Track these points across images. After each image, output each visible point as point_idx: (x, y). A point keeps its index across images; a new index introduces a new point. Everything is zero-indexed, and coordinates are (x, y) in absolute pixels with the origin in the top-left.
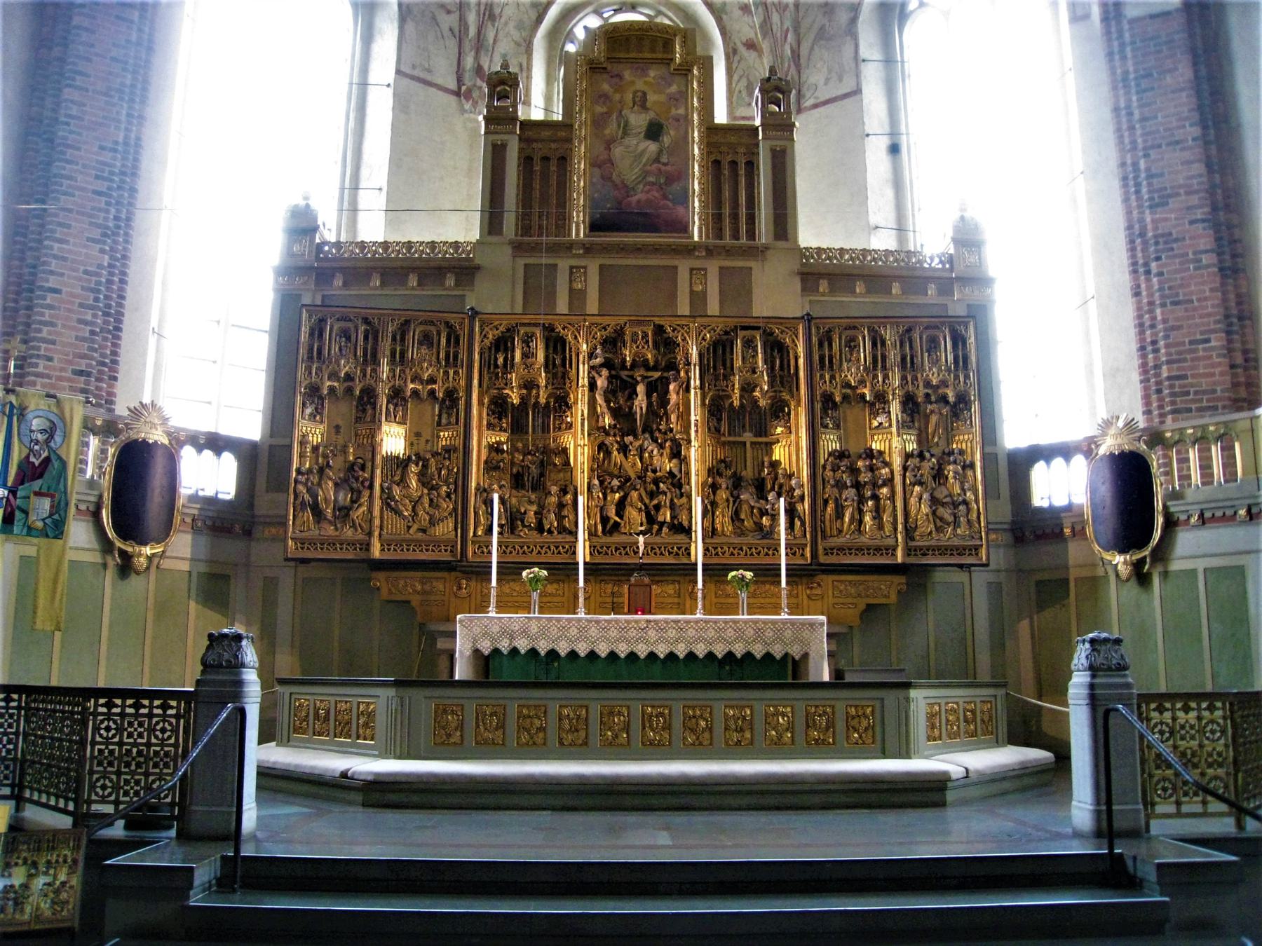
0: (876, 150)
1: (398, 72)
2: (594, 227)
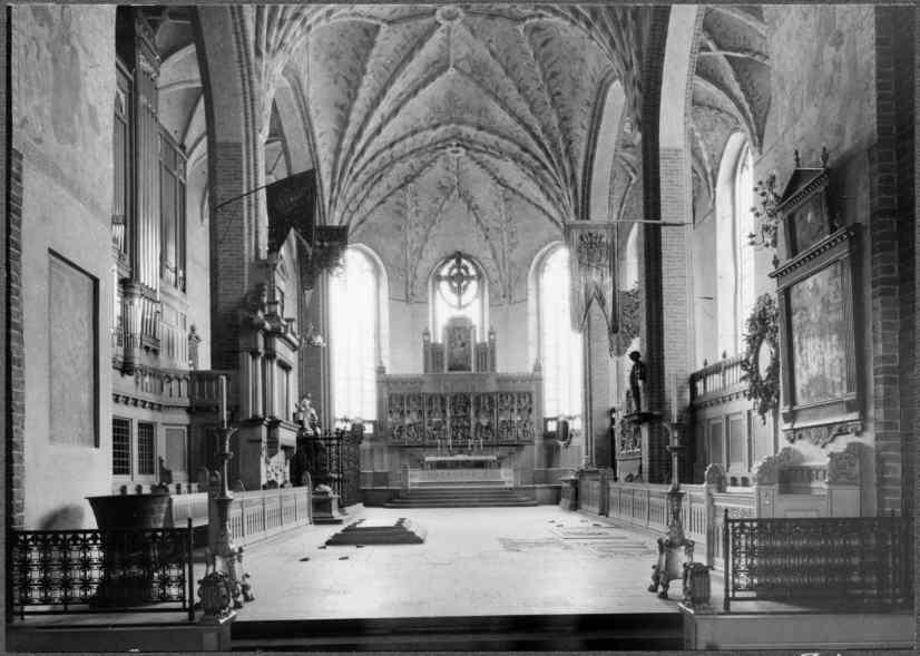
0: (532, 320)
1: (390, 298)
2: (450, 369)
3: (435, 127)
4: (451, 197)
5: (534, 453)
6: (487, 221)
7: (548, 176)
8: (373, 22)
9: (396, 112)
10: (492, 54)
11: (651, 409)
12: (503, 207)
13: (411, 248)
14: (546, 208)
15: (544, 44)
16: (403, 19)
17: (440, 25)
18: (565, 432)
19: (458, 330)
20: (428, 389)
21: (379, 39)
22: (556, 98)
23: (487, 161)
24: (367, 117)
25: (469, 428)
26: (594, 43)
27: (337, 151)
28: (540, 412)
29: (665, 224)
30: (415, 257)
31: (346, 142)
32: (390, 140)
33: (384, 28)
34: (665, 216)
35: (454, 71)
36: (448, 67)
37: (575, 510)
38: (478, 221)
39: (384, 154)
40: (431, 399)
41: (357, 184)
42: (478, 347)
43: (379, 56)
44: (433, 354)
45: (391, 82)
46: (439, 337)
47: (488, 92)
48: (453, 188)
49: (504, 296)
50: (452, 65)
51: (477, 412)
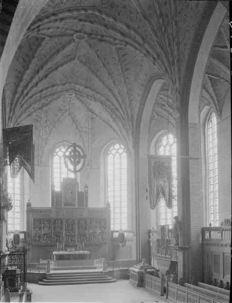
2: (65, 205)
3: (64, 84)
4: (65, 115)
6: (81, 127)
7: (119, 114)
8: (43, 36)
9: (46, 76)
10: (98, 57)
11: (184, 244)
12: (90, 121)
13: (41, 138)
14: (111, 124)
15: (123, 55)
16: (56, 36)
17: (74, 40)
19: (69, 185)
20: (53, 216)
21: (43, 43)
22: (127, 80)
23: (85, 100)
24: (32, 78)
25: (74, 236)
26: (155, 67)
27: (15, 92)
29: (191, 159)
30: (44, 143)
31: (20, 90)
32: (40, 89)
33: (47, 38)
34: (191, 154)
35: (78, 60)
36: (74, 59)
37: (140, 287)
38: (77, 127)
39: (37, 95)
40: (56, 221)
41: (22, 109)
43: (42, 50)
44: (56, 198)
45: (46, 63)
46: (58, 189)
47: (93, 72)
48: (66, 111)
49: (88, 165)
50: (77, 58)
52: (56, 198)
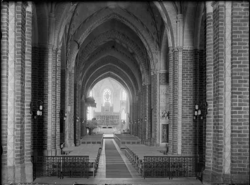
2: (106, 111)
5: (119, 125)
18: (124, 122)
19: (107, 104)
20: (102, 114)
28: (120, 119)
42: (110, 107)
44: (103, 108)
46: (104, 105)
51: (110, 119)
52: (103, 108)
